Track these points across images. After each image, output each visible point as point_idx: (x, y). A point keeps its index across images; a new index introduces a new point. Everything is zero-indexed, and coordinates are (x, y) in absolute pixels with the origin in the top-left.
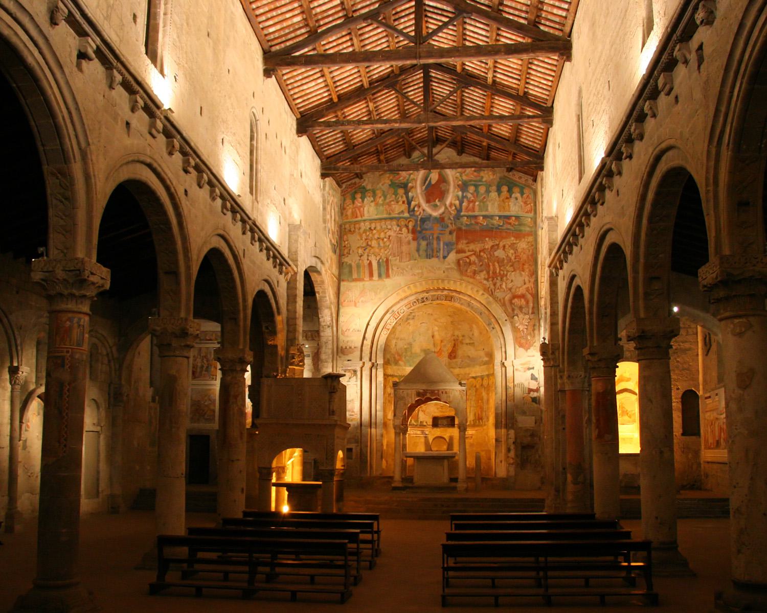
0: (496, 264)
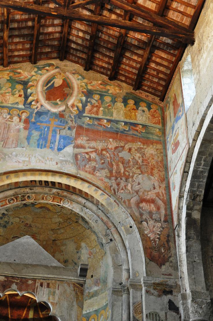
0: (121, 166)
